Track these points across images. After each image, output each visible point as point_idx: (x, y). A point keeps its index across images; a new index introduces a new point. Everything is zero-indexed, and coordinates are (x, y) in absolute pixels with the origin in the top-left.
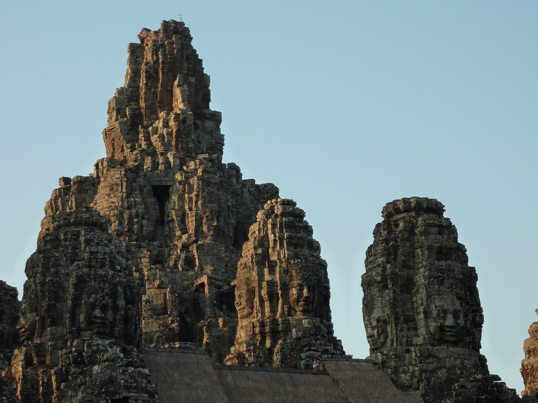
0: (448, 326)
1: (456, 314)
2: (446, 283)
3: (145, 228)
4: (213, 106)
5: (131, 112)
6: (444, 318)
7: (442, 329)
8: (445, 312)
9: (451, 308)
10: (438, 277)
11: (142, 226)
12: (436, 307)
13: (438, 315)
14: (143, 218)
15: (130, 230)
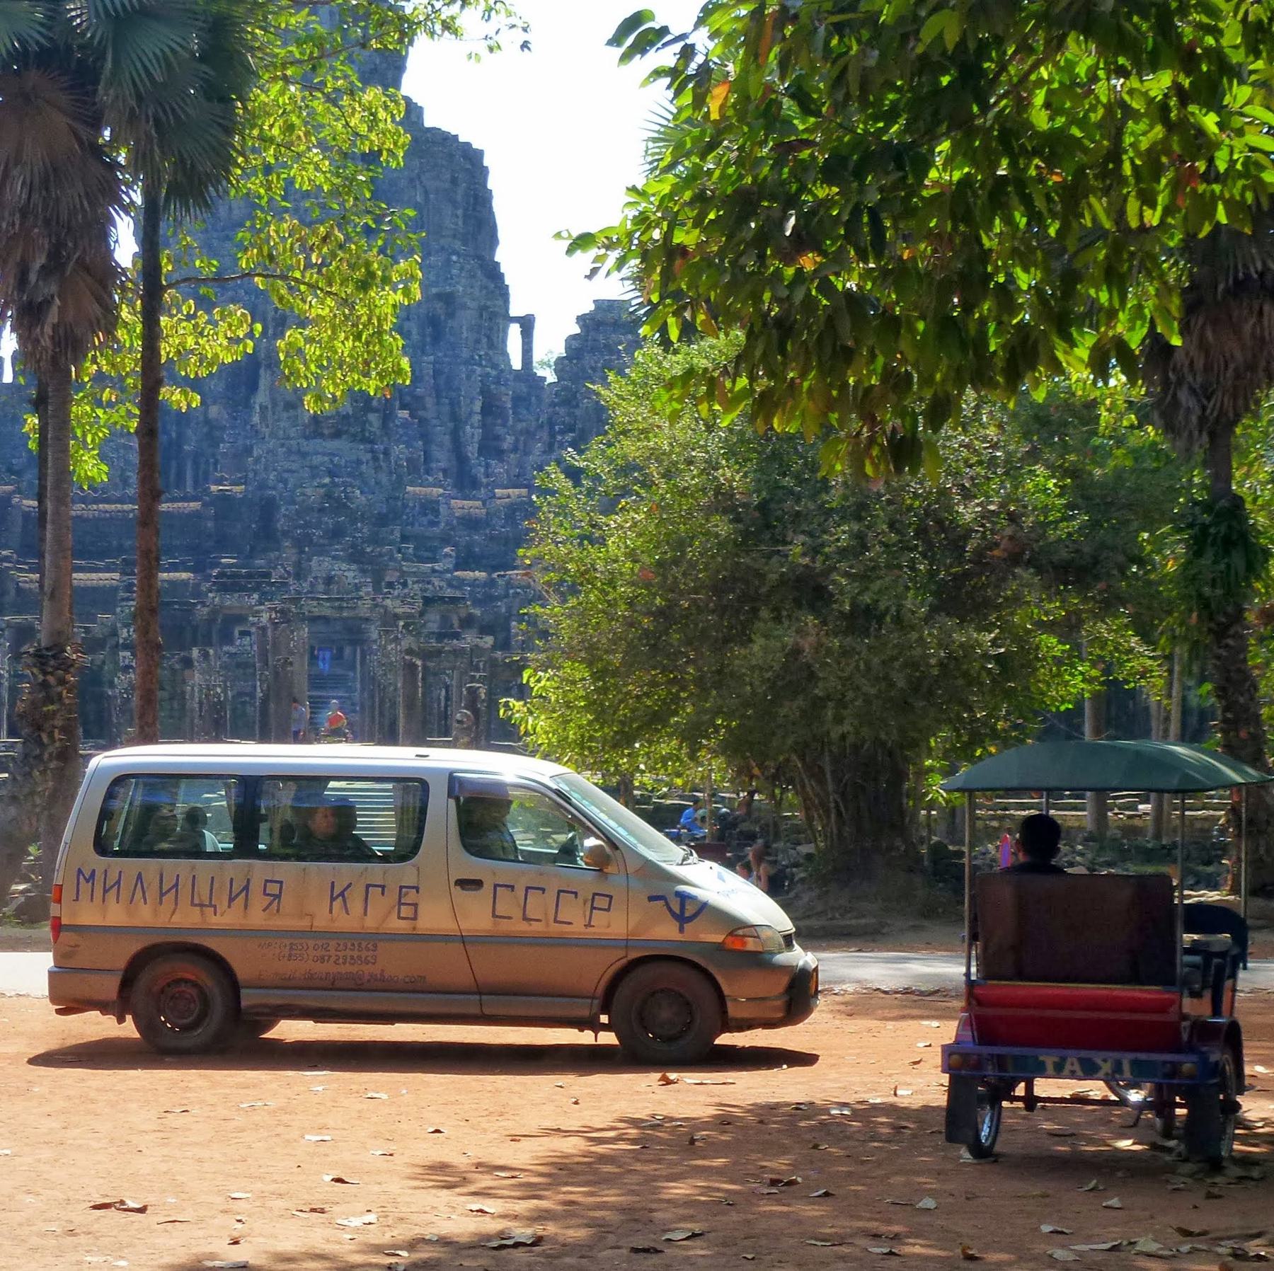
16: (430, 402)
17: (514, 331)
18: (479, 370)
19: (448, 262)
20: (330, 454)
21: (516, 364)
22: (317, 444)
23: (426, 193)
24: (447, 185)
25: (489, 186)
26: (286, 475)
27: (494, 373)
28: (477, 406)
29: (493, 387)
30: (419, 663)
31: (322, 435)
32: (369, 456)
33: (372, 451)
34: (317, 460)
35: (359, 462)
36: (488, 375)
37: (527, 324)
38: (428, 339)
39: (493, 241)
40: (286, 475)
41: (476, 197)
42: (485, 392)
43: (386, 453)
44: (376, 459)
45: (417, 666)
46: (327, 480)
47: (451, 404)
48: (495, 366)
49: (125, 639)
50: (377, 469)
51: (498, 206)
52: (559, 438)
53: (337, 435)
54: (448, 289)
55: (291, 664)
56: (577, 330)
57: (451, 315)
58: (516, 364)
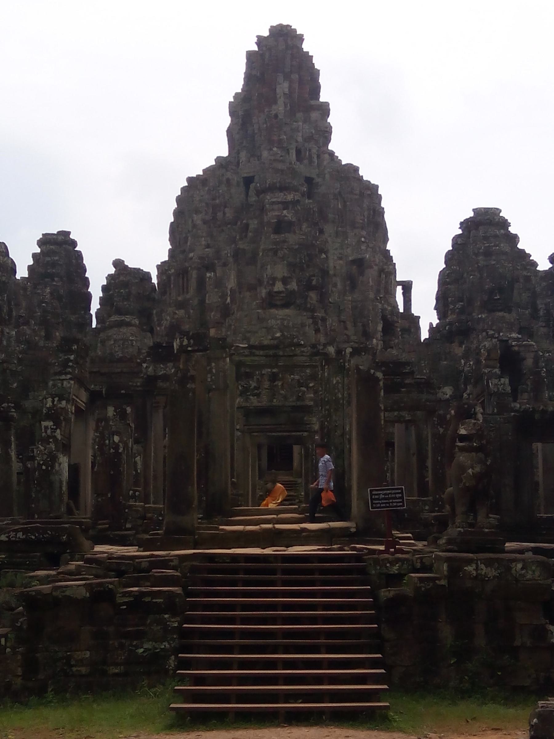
0: (276, 292)
1: (285, 281)
2: (280, 254)
3: (227, 215)
4: (322, 99)
5: (247, 114)
6: (273, 284)
7: (271, 295)
8: (273, 280)
9: (279, 275)
10: (271, 249)
11: (224, 214)
12: (267, 275)
13: (268, 282)
14: (225, 207)
15: (214, 218)
16: (349, 325)
17: (399, 290)
18: (380, 306)
19: (360, 242)
20: (281, 319)
21: (401, 310)
22: (274, 311)
23: (345, 202)
24: (357, 197)
25: (382, 205)
26: (248, 335)
27: (389, 308)
28: (380, 327)
29: (389, 316)
30: (380, 375)
31: (275, 306)
32: (311, 321)
33: (313, 317)
34: (272, 322)
35: (303, 325)
36: (386, 309)
37: (407, 287)
38: (347, 288)
39: (385, 239)
40: (248, 335)
41: (374, 211)
42: (384, 319)
43: (324, 320)
44: (315, 323)
45: (378, 380)
46: (278, 335)
47: (364, 326)
48: (389, 304)
49: (49, 409)
50: (317, 331)
51: (388, 218)
52: (451, 307)
53: (286, 305)
54: (360, 257)
55: (193, 378)
56: (460, 232)
57: (362, 273)
58: (401, 310)
